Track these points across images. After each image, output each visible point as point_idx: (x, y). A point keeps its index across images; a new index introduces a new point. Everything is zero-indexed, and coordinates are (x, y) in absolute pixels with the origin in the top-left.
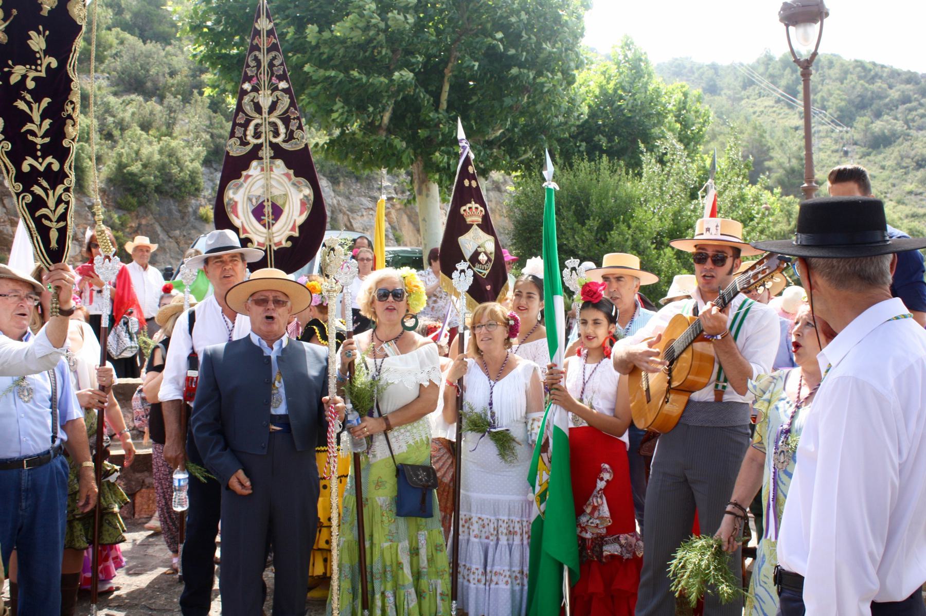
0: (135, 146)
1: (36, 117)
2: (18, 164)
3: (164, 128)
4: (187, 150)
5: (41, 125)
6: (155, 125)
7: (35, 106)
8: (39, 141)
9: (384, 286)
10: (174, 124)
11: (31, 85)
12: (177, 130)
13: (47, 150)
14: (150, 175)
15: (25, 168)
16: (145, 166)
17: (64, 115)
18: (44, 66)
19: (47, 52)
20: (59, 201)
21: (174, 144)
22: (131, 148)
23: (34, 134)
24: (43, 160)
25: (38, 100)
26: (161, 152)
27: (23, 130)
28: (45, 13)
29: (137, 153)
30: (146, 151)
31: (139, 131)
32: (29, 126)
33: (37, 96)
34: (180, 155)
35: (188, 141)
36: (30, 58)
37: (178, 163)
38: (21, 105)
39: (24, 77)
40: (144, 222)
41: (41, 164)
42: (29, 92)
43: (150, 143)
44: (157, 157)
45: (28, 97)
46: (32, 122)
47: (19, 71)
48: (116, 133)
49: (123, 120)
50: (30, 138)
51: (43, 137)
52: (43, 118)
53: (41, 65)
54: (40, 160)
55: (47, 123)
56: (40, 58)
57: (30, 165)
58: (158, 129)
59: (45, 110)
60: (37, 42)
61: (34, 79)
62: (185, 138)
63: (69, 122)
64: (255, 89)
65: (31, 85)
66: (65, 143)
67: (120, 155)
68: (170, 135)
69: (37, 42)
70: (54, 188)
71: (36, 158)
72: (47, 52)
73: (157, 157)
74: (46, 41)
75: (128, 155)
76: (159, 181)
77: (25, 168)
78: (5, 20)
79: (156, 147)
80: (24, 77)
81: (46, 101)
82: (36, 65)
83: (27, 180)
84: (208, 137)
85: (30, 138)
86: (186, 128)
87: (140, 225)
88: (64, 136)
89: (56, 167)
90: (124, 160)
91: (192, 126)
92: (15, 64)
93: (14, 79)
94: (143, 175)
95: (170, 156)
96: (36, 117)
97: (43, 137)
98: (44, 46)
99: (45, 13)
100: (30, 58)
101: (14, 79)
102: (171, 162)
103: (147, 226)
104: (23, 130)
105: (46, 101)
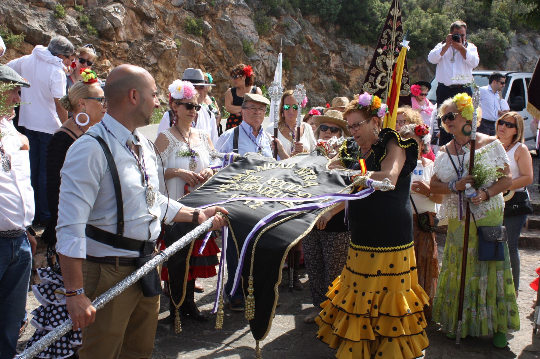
0: (417, 19)
3: (436, 8)
4: (449, 21)
6: (431, 5)
10: (443, 4)
12: (445, 8)
14: (425, 37)
16: (422, 31)
21: (441, 17)
22: (415, 20)
26: (433, 23)
29: (418, 23)
30: (424, 22)
31: (420, 10)
34: (444, 24)
35: (450, 15)
37: (443, 29)
40: (420, 66)
43: (427, 17)
44: (430, 26)
48: (407, 12)
49: (411, 3)
58: (433, 8)
62: (449, 13)
64: (384, 53)
67: (408, 25)
68: (440, 12)
73: (430, 26)
75: (413, 25)
76: (431, 41)
79: (430, 20)
84: (463, 12)
86: (449, 7)
87: (418, 67)
90: (410, 28)
91: (454, 6)
94: (421, 37)
95: (438, 25)
102: (438, 28)
103: (422, 68)
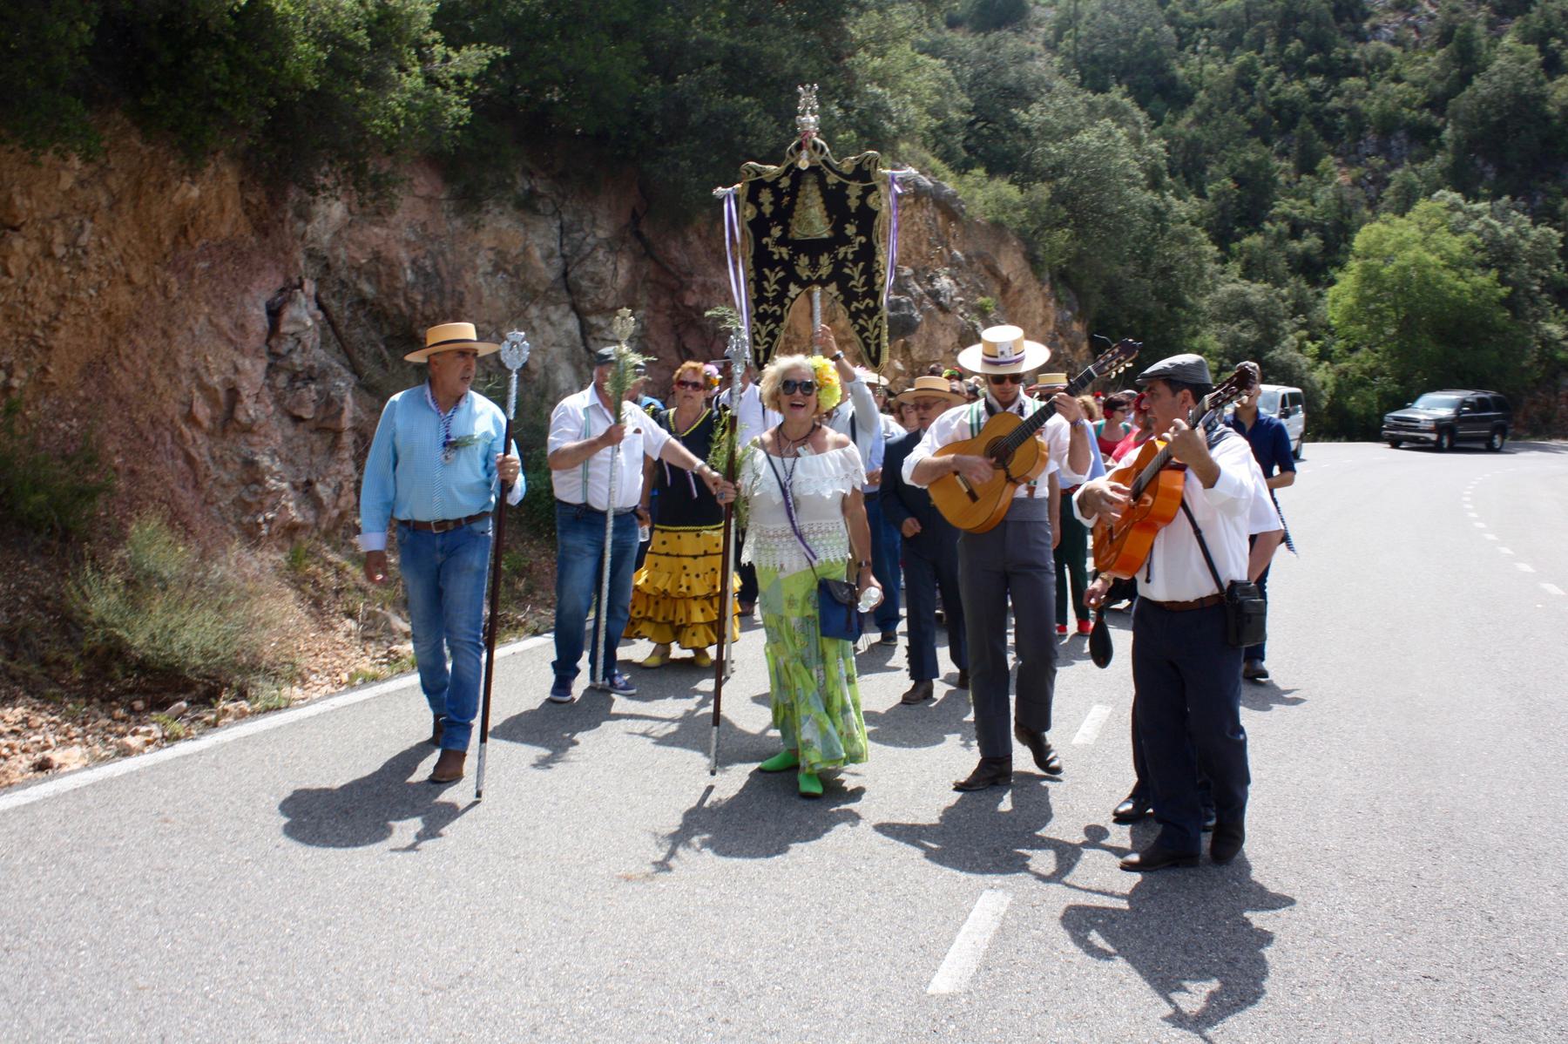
9: (790, 378)
11: (850, 257)
13: (865, 295)
19: (857, 234)
20: (875, 326)
25: (856, 265)
33: (855, 262)
36: (847, 241)
38: (847, 271)
46: (852, 278)
47: (842, 250)
55: (862, 279)
60: (850, 230)
65: (850, 257)
69: (850, 230)
70: (871, 317)
72: (857, 234)
81: (861, 265)
83: (855, 316)
89: (872, 304)
93: (840, 256)
100: (847, 241)
101: (840, 256)
105: (861, 265)
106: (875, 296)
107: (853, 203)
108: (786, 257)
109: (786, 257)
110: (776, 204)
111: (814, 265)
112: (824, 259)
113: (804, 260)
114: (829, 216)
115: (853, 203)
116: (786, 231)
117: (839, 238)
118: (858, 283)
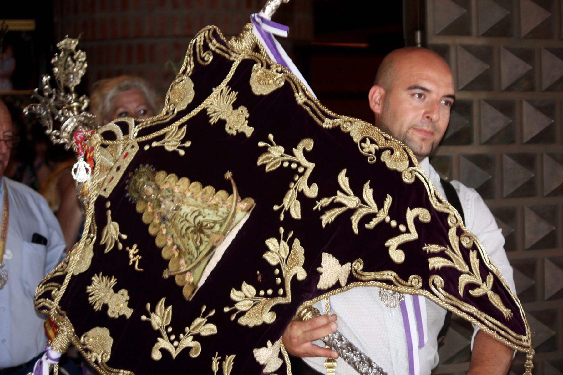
1: (351, 202)
2: (390, 265)
5: (363, 202)
7: (340, 197)
8: (383, 215)
11: (312, 192)
15: (398, 257)
17: (372, 160)
18: (304, 162)
19: (289, 151)
23: (369, 217)
24: (406, 224)
25: (335, 188)
27: (356, 231)
28: (249, 131)
32: (355, 220)
33: (329, 187)
38: (327, 218)
39: (301, 196)
41: (408, 231)
42: (319, 198)
45: (325, 202)
50: (372, 225)
51: (380, 206)
52: (358, 192)
53: (299, 165)
54: (402, 228)
55: (368, 193)
56: (291, 162)
57: (399, 247)
59: (352, 186)
61: (309, 184)
63: (385, 157)
65: (312, 192)
66: (408, 179)
71: (396, 232)
74: (278, 144)
77: (398, 257)
78: (230, 192)
80: (301, 196)
81: (343, 180)
82: (295, 171)
85: (372, 225)
88: (397, 174)
92: (280, 202)
93: (296, 213)
96: (351, 202)
97: (380, 206)
98: (282, 149)
99: (249, 131)
101: (296, 213)
104: (356, 231)
105: (343, 180)
106: (416, 194)
107: (238, 122)
108: (210, 329)
109: (210, 329)
110: (125, 278)
111: (268, 279)
112: (276, 251)
113: (244, 296)
114: (221, 185)
115: (238, 122)
116: (172, 291)
117: (265, 189)
118: (359, 204)
